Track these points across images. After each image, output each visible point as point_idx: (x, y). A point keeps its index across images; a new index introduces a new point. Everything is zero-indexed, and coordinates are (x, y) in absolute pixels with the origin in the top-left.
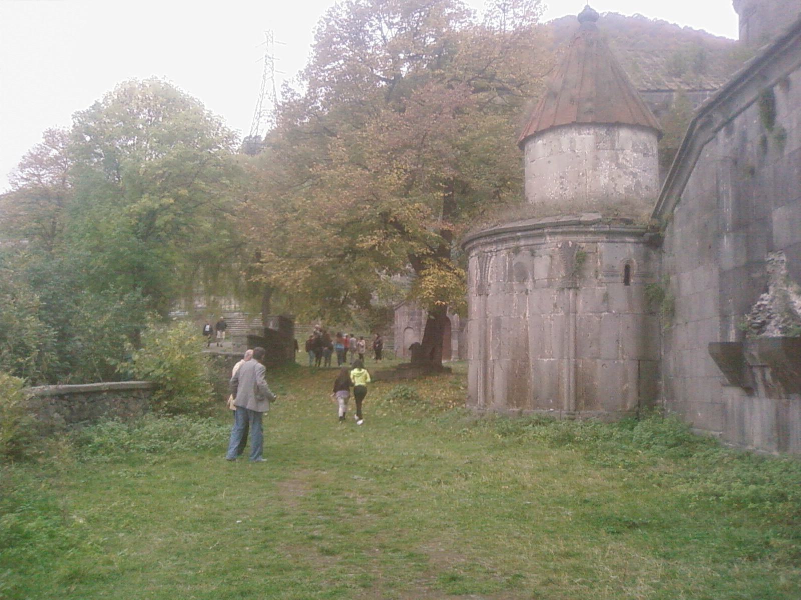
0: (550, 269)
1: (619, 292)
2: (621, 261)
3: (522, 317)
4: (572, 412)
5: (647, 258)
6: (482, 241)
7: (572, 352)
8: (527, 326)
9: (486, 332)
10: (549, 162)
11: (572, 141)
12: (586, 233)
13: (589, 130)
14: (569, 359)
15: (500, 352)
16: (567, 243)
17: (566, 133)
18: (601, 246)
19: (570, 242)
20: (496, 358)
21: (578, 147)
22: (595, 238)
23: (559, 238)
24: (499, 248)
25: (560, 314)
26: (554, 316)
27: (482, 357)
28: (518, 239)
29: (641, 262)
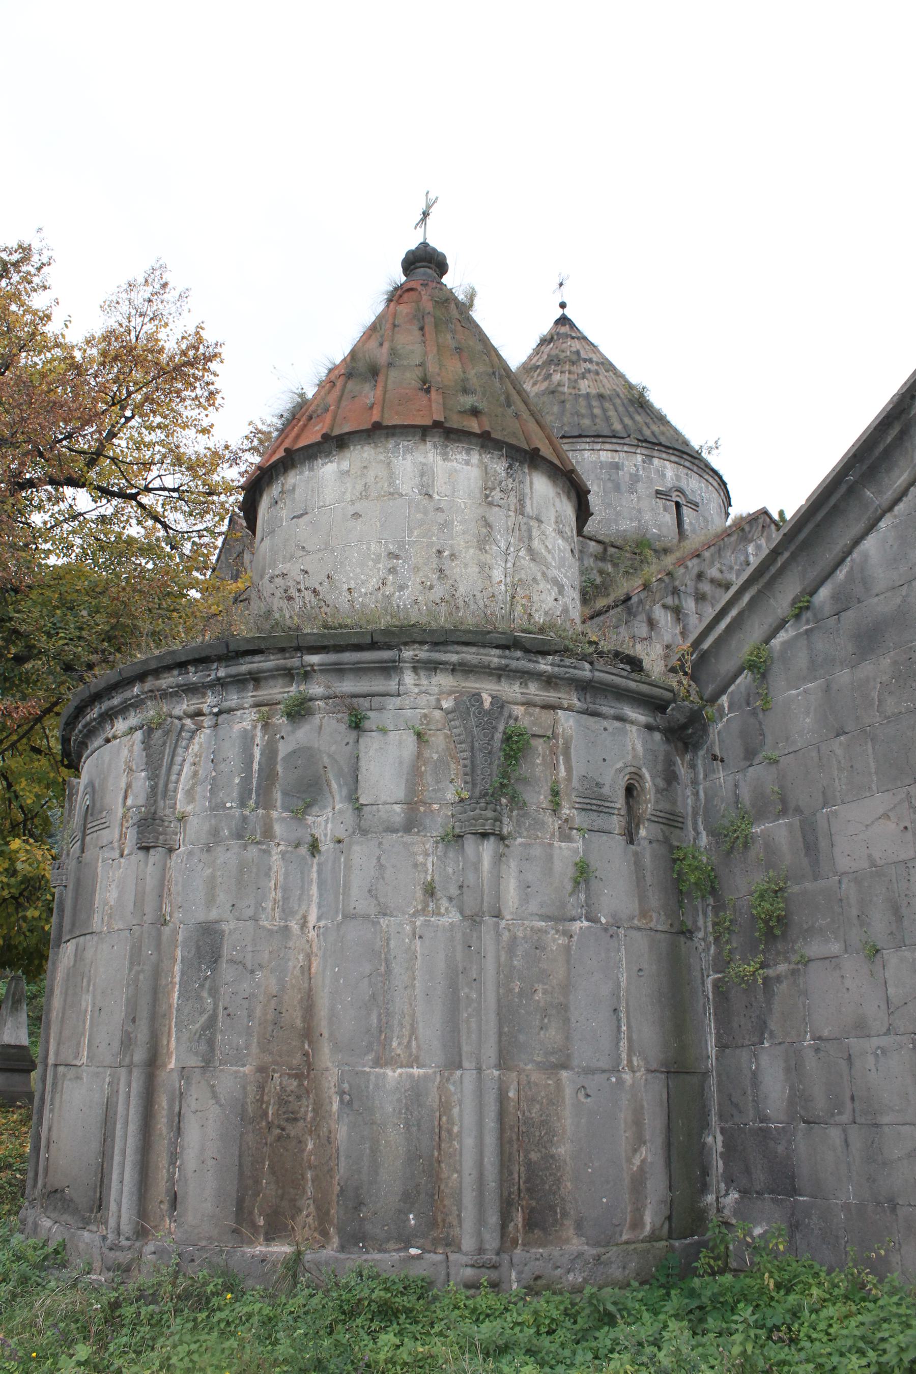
0: (415, 775)
1: (613, 858)
2: (620, 770)
3: (295, 927)
4: (490, 1256)
5: (670, 777)
6: (168, 681)
7: (490, 1052)
8: (309, 957)
9: (157, 973)
10: (356, 515)
11: (424, 472)
12: (525, 676)
13: (468, 453)
14: (479, 1069)
15: (211, 1043)
16: (477, 697)
17: (408, 451)
18: (567, 722)
19: (485, 696)
20: (193, 1061)
21: (440, 487)
22: (551, 696)
23: (444, 680)
24: (226, 705)
25: (445, 920)
26: (427, 924)
27: (139, 1055)
28: (307, 675)
29: (661, 783)
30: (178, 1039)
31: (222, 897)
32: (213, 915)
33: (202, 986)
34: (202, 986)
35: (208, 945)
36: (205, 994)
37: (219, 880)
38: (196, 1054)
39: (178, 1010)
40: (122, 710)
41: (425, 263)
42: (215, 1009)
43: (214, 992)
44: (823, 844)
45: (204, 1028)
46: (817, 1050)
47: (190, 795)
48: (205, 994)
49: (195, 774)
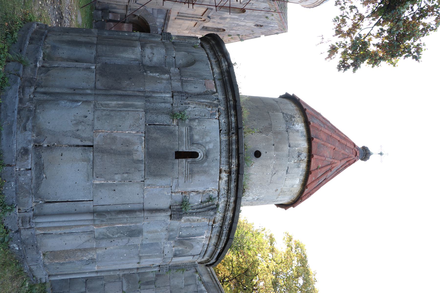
15: (103, 239)
20: (96, 234)
30: (104, 228)
31: (150, 235)
32: (145, 234)
33: (122, 233)
34: (122, 233)
35: (135, 233)
36: (119, 235)
37: (156, 234)
38: (99, 235)
39: (113, 227)
40: (229, 182)
41: (365, 154)
42: (114, 238)
43: (119, 237)
44: (148, 287)
45: (108, 236)
46: (102, 285)
47: (188, 220)
48: (119, 235)
49: (194, 221)
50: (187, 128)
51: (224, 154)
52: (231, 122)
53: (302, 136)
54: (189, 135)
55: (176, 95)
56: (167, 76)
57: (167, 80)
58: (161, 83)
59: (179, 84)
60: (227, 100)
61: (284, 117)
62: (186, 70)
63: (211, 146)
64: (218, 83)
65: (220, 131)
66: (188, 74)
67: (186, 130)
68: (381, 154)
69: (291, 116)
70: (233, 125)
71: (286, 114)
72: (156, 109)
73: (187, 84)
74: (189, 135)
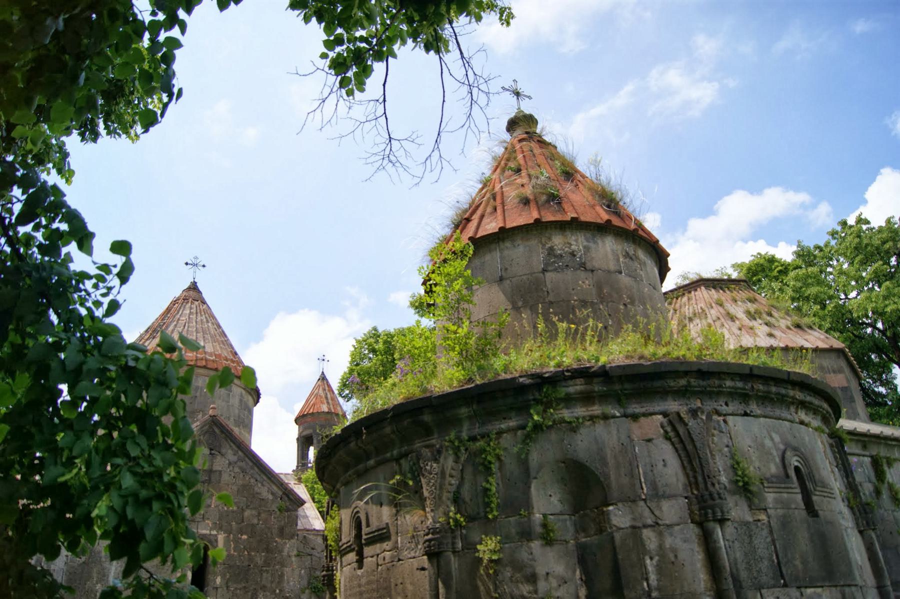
50: (766, 490)
51: (778, 412)
52: (733, 388)
53: (595, 243)
54: (778, 485)
55: (722, 512)
56: (648, 535)
57: (660, 534)
58: (674, 551)
59: (666, 505)
60: (683, 393)
61: (555, 270)
62: (614, 484)
63: (777, 438)
64: (635, 408)
65: (746, 414)
66: (625, 480)
67: (771, 490)
68: (517, 94)
69: (549, 254)
70: (740, 384)
71: (546, 264)
72: (748, 563)
73: (660, 485)
74: (778, 485)
